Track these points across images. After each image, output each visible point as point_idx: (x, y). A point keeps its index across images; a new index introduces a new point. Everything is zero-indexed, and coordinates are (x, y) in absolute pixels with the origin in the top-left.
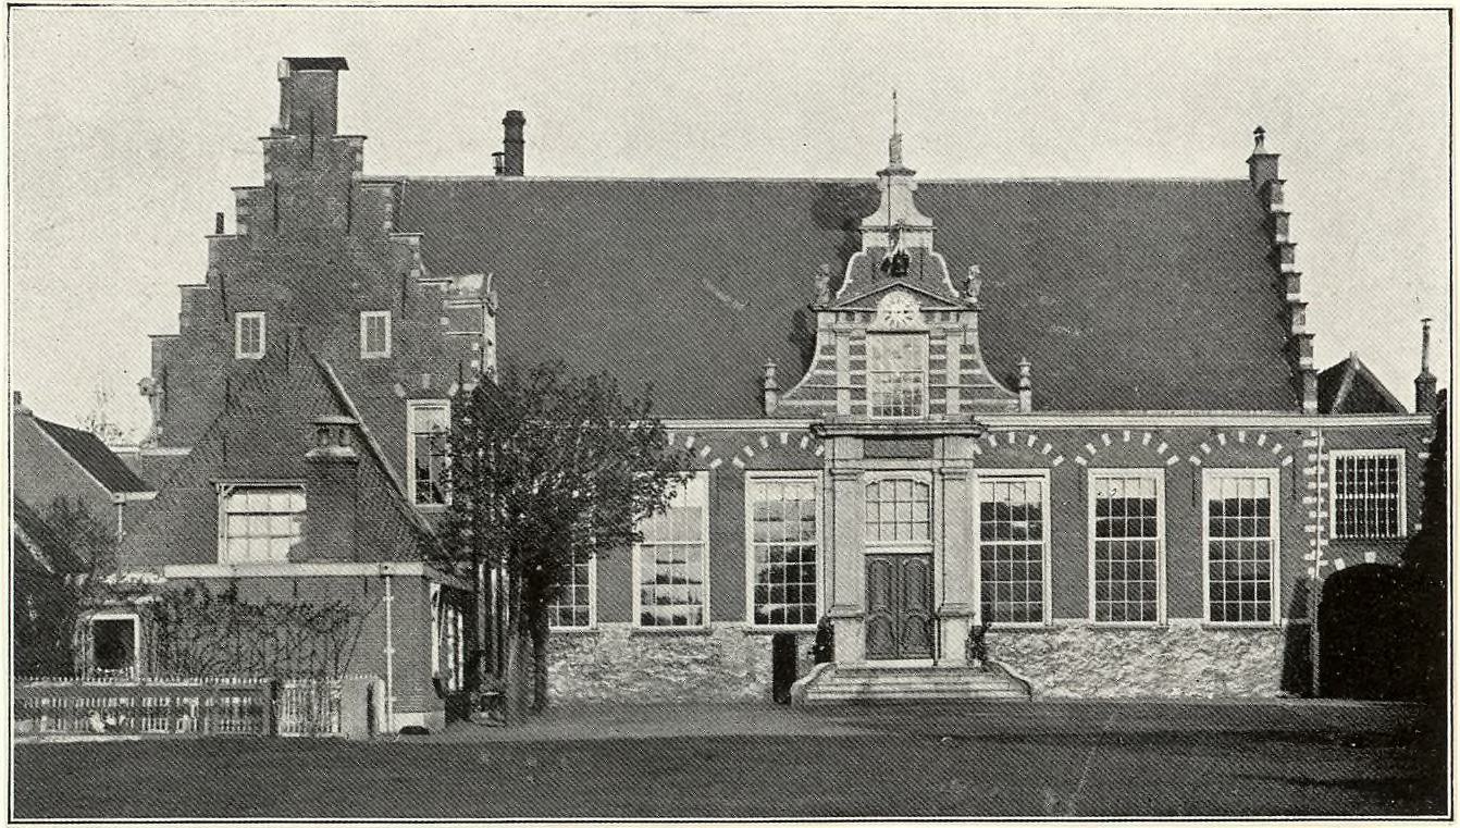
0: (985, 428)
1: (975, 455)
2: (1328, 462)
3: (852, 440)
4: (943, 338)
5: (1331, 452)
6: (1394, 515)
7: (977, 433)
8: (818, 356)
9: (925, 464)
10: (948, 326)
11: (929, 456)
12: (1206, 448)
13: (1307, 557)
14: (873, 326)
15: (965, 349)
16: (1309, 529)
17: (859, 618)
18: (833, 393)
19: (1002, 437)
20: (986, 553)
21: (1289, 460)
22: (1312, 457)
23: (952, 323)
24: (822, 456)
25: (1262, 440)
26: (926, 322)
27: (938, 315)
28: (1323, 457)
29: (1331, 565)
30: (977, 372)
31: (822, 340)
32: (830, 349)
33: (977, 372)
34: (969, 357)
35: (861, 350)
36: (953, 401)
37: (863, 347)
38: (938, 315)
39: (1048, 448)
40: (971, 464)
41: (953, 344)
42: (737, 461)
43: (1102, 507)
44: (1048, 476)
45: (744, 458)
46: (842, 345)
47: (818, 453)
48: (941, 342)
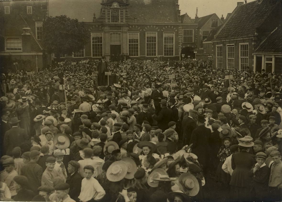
0: (130, 25)
1: (128, 29)
2: (182, 31)
4: (123, 10)
5: (183, 29)
6: (192, 39)
7: (128, 26)
9: (120, 30)
10: (123, 8)
11: (120, 29)
13: (179, 46)
14: (111, 7)
15: (126, 12)
16: (179, 41)
17: (109, 56)
18: (105, 19)
19: (132, 26)
20: (130, 45)
21: (176, 30)
22: (180, 30)
23: (124, 7)
25: (172, 27)
26: (120, 7)
27: (122, 6)
28: (182, 30)
29: (183, 47)
30: (128, 15)
33: (128, 15)
34: (127, 13)
35: (109, 11)
36: (124, 20)
38: (122, 6)
39: (139, 28)
40: (127, 31)
41: (124, 11)
42: (89, 30)
43: (148, 38)
44: (139, 32)
45: (90, 29)
47: (103, 28)
48: (122, 10)
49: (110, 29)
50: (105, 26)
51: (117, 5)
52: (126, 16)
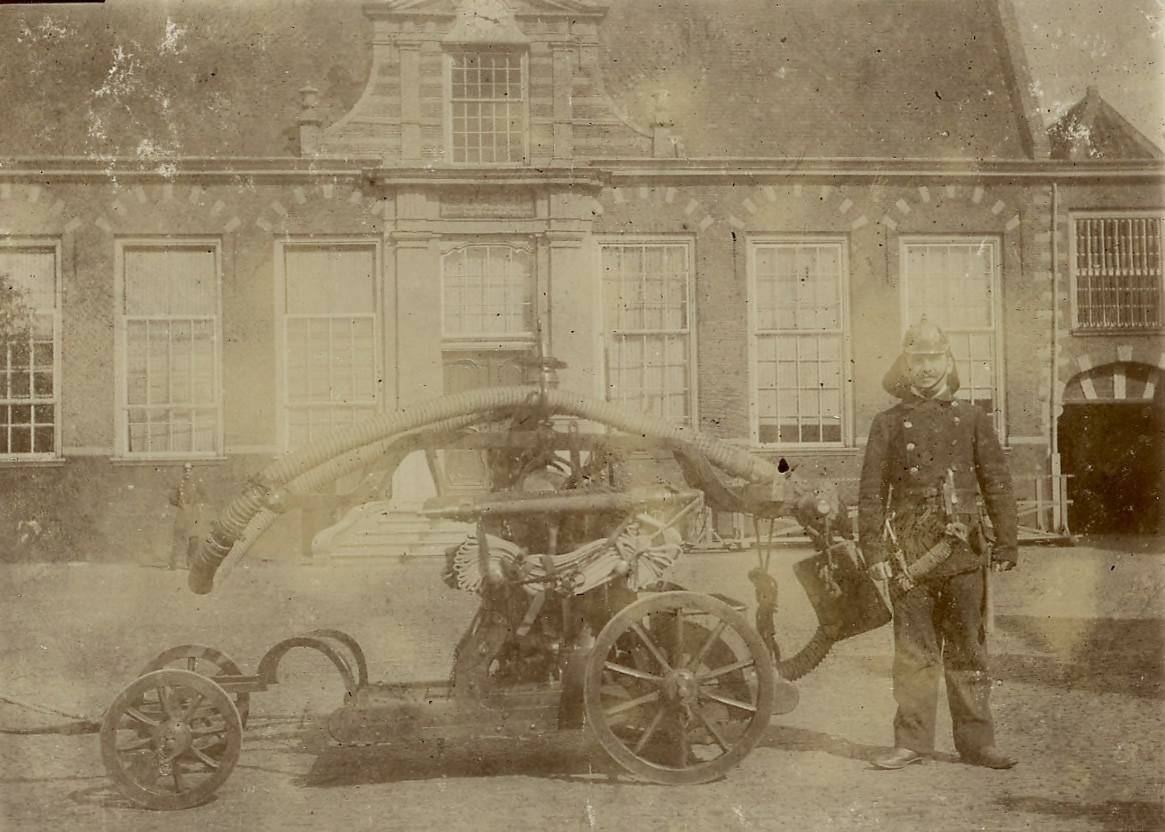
3: (419, 199)
4: (551, 54)
8: (374, 77)
12: (902, 205)
21: (1013, 224)
23: (564, 32)
24: (380, 217)
31: (381, 55)
32: (391, 69)
37: (439, 65)
38: (542, 26)
40: (588, 227)
46: (410, 61)
47: (375, 212)
48: (545, 61)
49: (442, 218)
50: (396, 189)
51: (496, 21)
52: (577, 111)
